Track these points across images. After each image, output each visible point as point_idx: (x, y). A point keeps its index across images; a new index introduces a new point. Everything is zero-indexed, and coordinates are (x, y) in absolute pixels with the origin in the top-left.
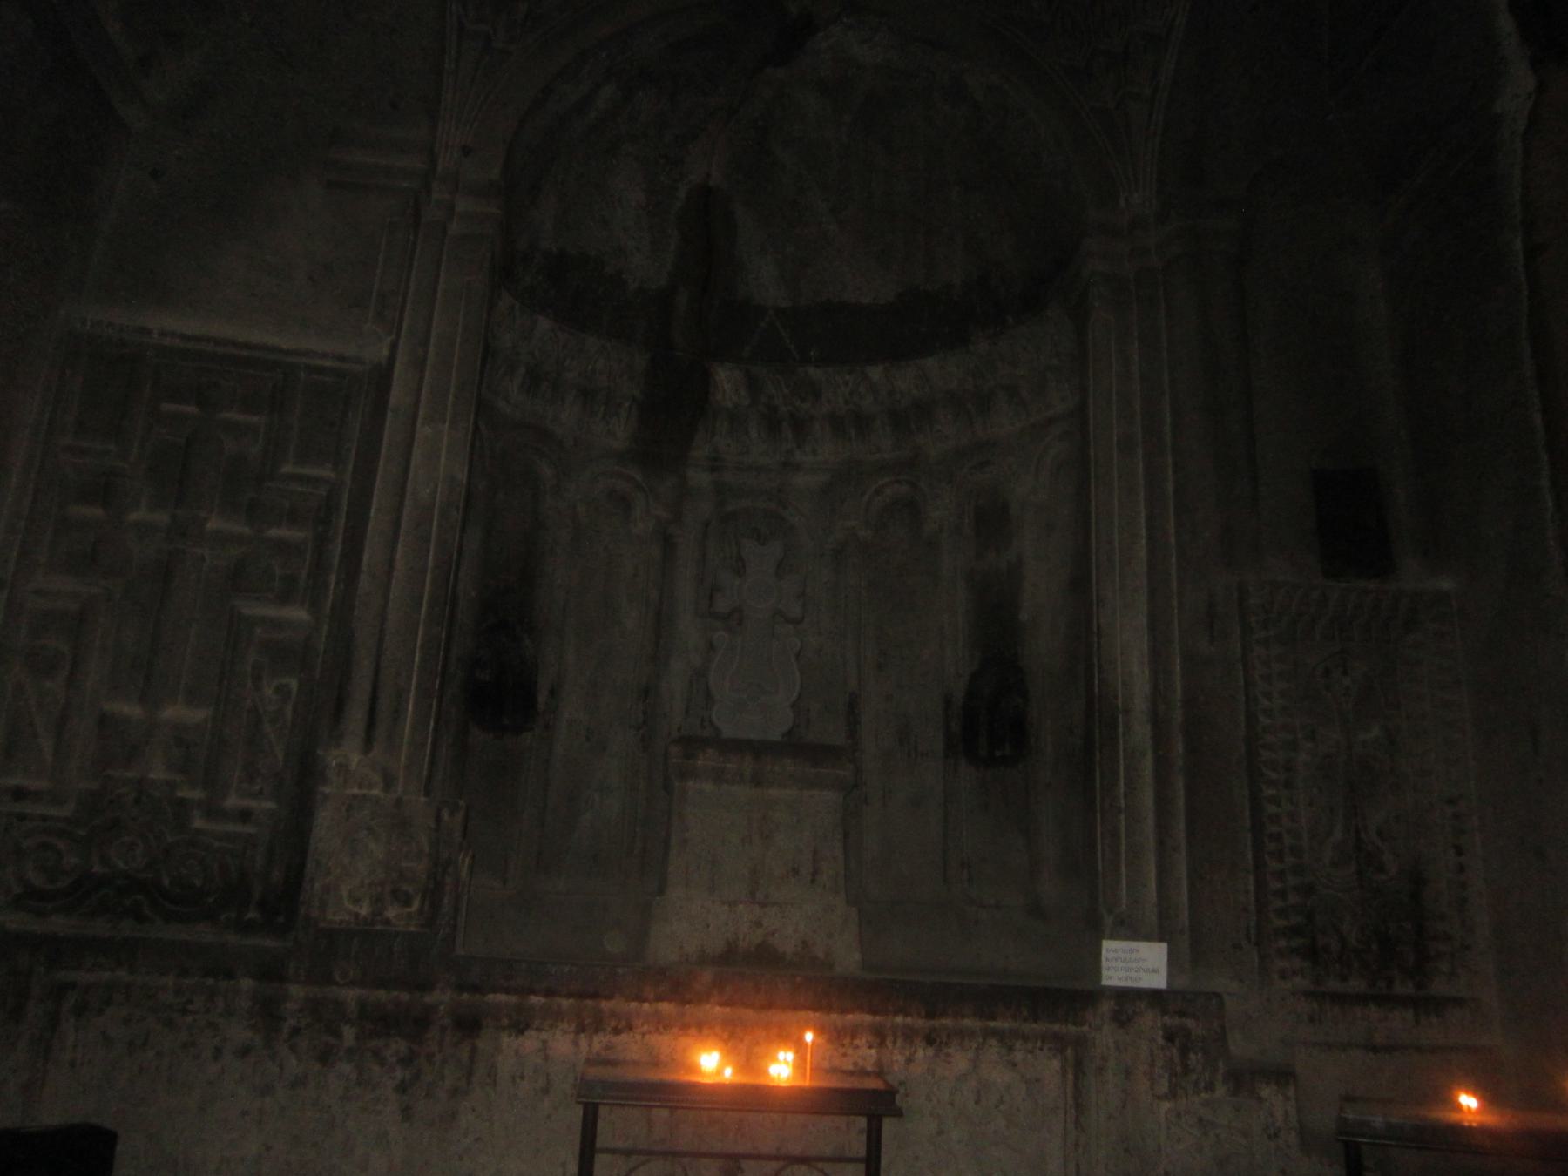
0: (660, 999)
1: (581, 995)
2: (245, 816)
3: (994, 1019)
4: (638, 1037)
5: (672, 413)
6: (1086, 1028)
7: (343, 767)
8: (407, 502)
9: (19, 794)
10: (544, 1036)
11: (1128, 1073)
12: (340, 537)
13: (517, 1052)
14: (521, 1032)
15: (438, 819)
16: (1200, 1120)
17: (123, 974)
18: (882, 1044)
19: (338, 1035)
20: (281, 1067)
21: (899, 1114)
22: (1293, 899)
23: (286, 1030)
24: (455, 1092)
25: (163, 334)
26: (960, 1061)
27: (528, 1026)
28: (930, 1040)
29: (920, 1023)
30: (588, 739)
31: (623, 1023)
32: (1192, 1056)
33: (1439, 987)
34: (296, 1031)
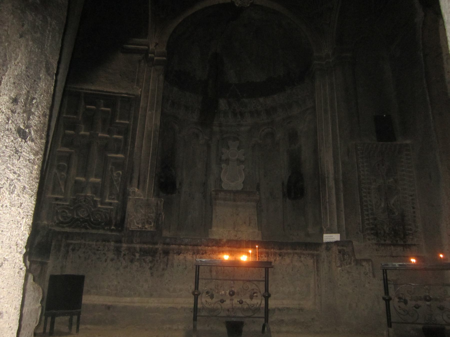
0: (213, 246)
1: (194, 245)
2: (110, 204)
5: (209, 112)
7: (134, 192)
9: (57, 199)
10: (185, 255)
11: (330, 262)
14: (179, 254)
15: (157, 204)
16: (348, 272)
17: (83, 241)
18: (268, 256)
19: (135, 256)
20: (121, 263)
21: (272, 267)
22: (371, 221)
23: (122, 255)
24: (163, 269)
25: (86, 90)
26: (288, 260)
27: (181, 253)
28: (280, 255)
29: (278, 251)
32: (345, 256)
33: (409, 242)
34: (125, 255)
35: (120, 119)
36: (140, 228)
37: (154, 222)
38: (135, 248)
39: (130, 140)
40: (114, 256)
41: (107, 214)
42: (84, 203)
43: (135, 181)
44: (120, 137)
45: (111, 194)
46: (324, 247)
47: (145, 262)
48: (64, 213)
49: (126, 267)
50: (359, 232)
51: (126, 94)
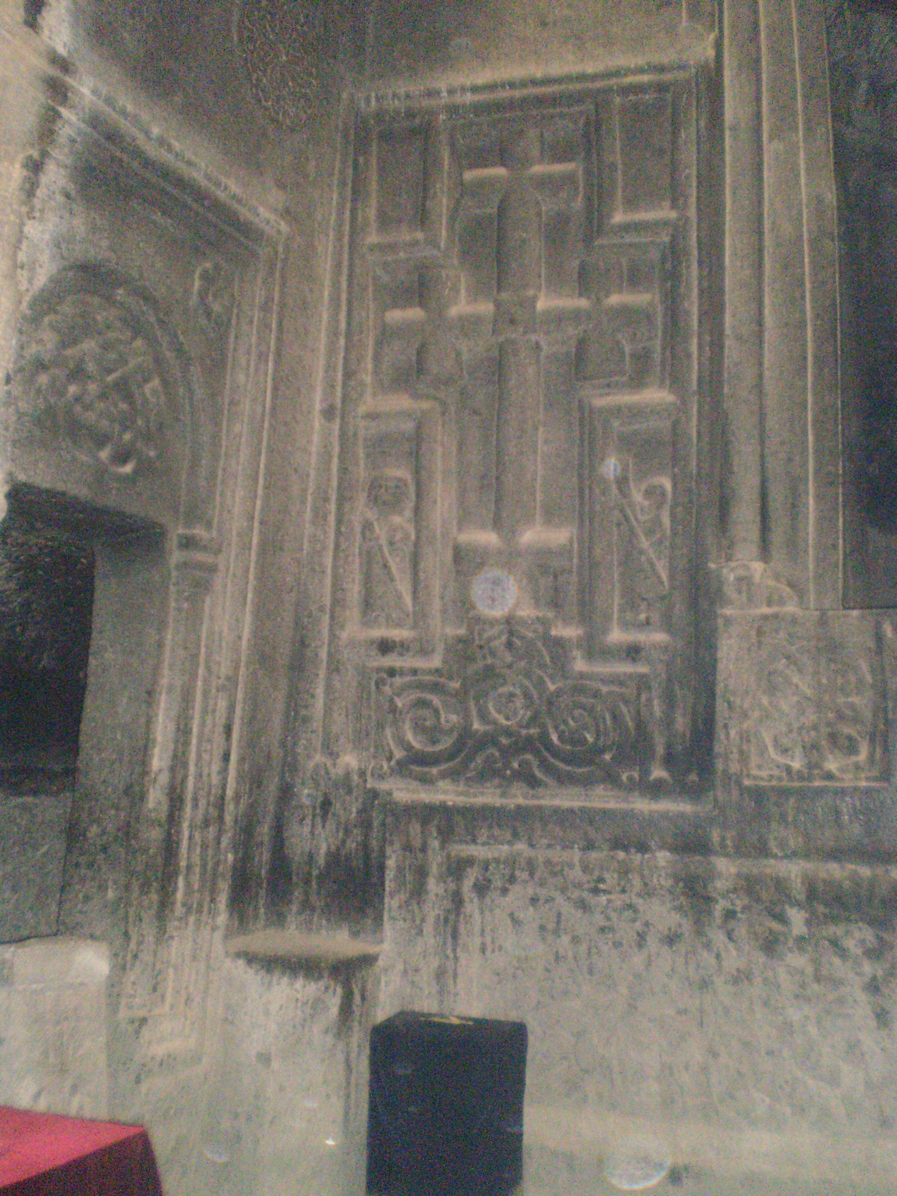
7: (745, 581)
8: (768, 242)
9: (385, 647)
12: (695, 292)
15: (879, 638)
19: (782, 919)
20: (718, 956)
25: (451, 92)
34: (730, 915)
35: (631, 203)
36: (801, 778)
37: (872, 741)
38: (780, 885)
39: (693, 306)
40: (676, 917)
41: (624, 709)
42: (509, 659)
44: (641, 299)
45: (631, 600)
47: (843, 953)
48: (426, 712)
49: (741, 977)
51: (640, 71)
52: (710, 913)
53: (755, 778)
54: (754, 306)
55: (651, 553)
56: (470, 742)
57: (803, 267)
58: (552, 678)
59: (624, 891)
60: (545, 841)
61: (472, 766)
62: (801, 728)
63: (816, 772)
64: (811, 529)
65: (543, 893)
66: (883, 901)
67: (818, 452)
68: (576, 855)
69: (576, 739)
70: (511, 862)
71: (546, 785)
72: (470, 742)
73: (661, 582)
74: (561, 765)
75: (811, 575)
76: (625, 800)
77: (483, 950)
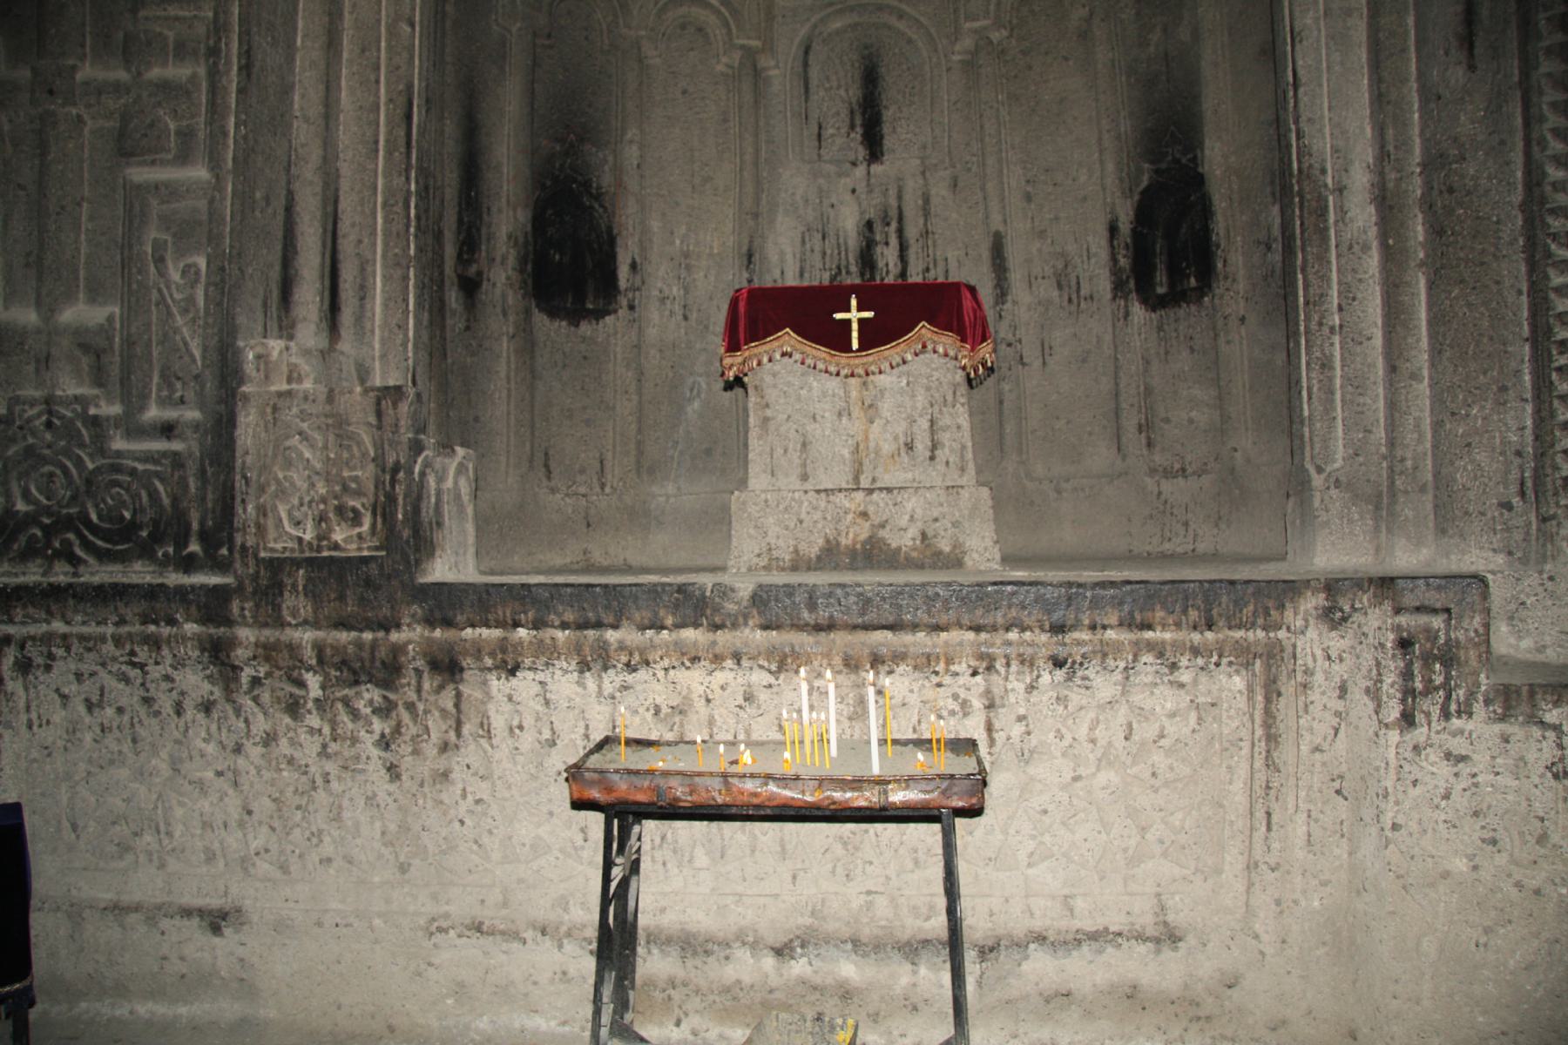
1: (582, 626)
2: (167, 430)
3: (1150, 627)
4: (660, 674)
6: (1282, 634)
10: (540, 676)
11: (1343, 690)
13: (510, 699)
14: (512, 672)
17: (58, 626)
18: (990, 668)
19: (301, 684)
24: (445, 747)
26: (1105, 685)
28: (1058, 663)
30: (686, 318)
31: (637, 658)
34: (256, 681)
37: (374, 514)
38: (293, 648)
40: (207, 686)
42: (48, 436)
43: (309, 298)
46: (1312, 602)
47: (355, 715)
50: (1516, 501)
52: (237, 679)
53: (273, 550)
54: (322, 87)
55: (186, 332)
56: (12, 523)
57: (379, 50)
58: (91, 456)
59: (157, 663)
60: (79, 618)
61: (16, 547)
62: (310, 502)
63: (325, 543)
64: (378, 310)
65: (85, 668)
66: (383, 663)
67: (387, 234)
68: (110, 630)
69: (112, 516)
70: (48, 639)
71: (85, 562)
72: (12, 523)
73: (194, 361)
74: (100, 543)
75: (377, 355)
76: (161, 574)
77: (30, 727)
